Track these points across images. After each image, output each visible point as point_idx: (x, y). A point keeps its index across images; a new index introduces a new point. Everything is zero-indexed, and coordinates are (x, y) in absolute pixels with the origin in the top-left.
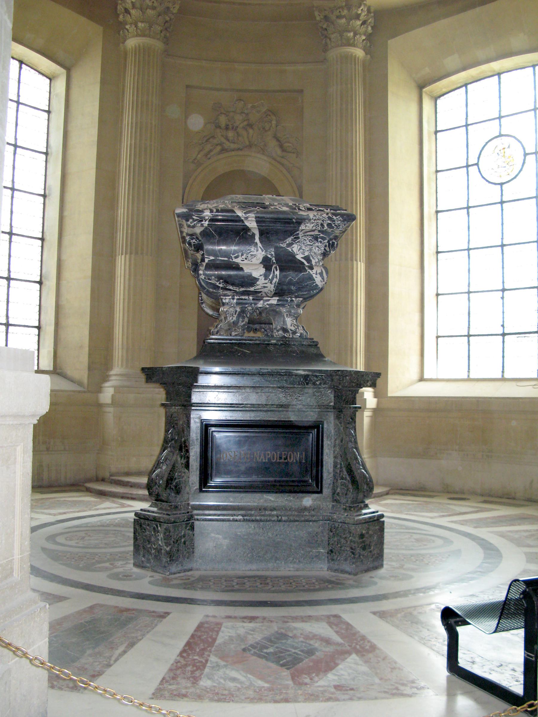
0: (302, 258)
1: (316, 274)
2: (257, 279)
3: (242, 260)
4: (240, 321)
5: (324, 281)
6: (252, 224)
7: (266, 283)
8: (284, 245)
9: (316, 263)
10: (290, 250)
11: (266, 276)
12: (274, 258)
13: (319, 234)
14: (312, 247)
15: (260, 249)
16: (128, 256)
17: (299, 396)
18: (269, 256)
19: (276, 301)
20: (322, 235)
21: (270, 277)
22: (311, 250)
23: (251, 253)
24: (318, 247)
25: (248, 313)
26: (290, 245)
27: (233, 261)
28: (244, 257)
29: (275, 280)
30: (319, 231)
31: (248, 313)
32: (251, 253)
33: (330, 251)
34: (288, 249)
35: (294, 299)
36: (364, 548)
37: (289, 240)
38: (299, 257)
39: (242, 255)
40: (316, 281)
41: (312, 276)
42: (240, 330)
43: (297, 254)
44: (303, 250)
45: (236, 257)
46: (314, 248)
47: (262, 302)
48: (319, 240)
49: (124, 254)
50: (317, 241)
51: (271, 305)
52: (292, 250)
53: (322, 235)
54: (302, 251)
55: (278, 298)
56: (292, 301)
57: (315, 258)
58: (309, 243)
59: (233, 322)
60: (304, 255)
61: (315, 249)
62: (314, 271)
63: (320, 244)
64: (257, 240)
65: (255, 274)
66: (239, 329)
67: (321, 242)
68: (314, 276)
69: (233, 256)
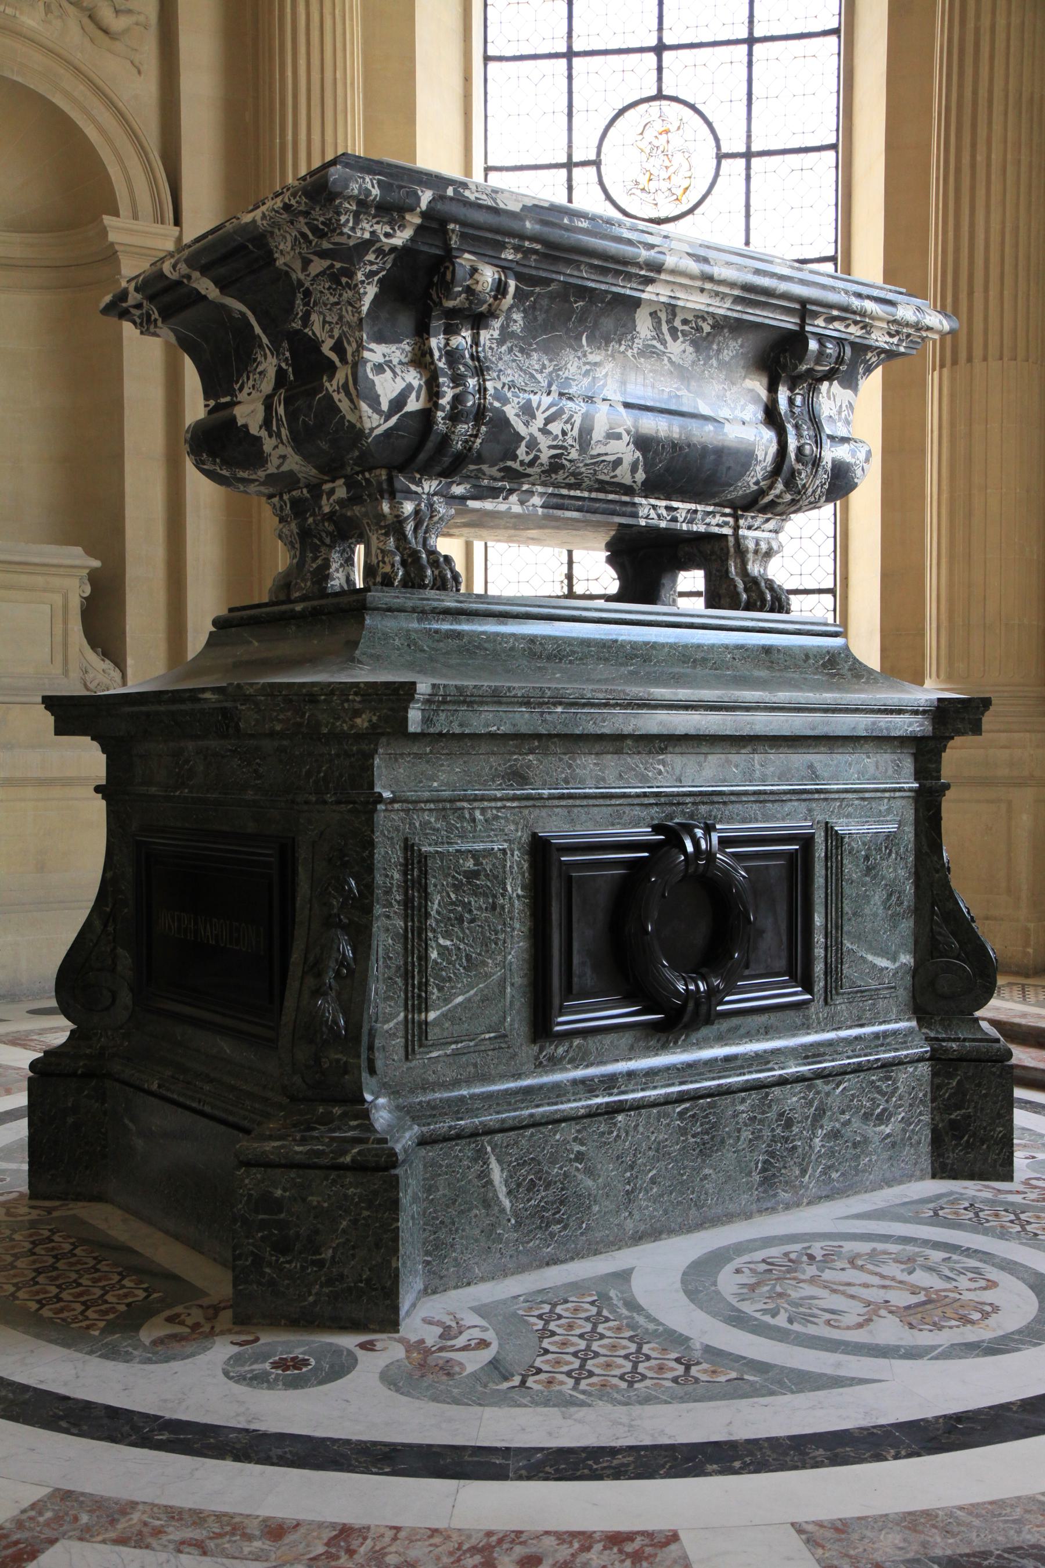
0: (331, 349)
1: (339, 393)
2: (258, 440)
3: (249, 394)
4: (308, 560)
5: (356, 408)
6: (206, 287)
7: (276, 447)
8: (297, 325)
9: (353, 355)
10: (310, 333)
11: (267, 423)
12: (290, 369)
13: (328, 262)
14: (341, 309)
15: (267, 351)
16: (945, 371)
17: (259, 765)
18: (283, 365)
19: (344, 489)
20: (338, 265)
21: (275, 428)
22: (341, 318)
23: (260, 369)
24: (351, 304)
25: (324, 535)
26: (306, 319)
27: (239, 399)
28: (251, 383)
29: (282, 430)
30: (323, 254)
31: (324, 535)
32: (260, 369)
33: (440, 298)
34: (306, 331)
35: (367, 475)
36: (283, 1247)
37: (300, 308)
38: (326, 349)
39: (248, 379)
40: (344, 412)
41: (331, 398)
42: (309, 583)
43: (323, 342)
44: (330, 323)
45: (241, 389)
46: (344, 313)
47: (325, 497)
48: (344, 280)
49: (938, 368)
50: (339, 283)
51: (341, 502)
52: (314, 334)
53: (338, 265)
54: (327, 326)
55: (341, 481)
56: (367, 480)
57: (352, 339)
58: (333, 300)
59: (297, 563)
60: (331, 337)
61: (347, 311)
62: (334, 382)
63: (350, 293)
64: (258, 330)
65: (254, 430)
66: (304, 580)
67: (348, 285)
68: (336, 397)
69: (237, 387)
